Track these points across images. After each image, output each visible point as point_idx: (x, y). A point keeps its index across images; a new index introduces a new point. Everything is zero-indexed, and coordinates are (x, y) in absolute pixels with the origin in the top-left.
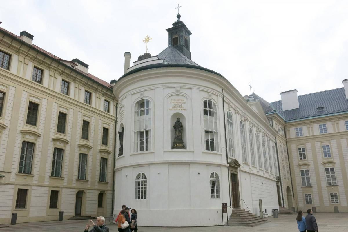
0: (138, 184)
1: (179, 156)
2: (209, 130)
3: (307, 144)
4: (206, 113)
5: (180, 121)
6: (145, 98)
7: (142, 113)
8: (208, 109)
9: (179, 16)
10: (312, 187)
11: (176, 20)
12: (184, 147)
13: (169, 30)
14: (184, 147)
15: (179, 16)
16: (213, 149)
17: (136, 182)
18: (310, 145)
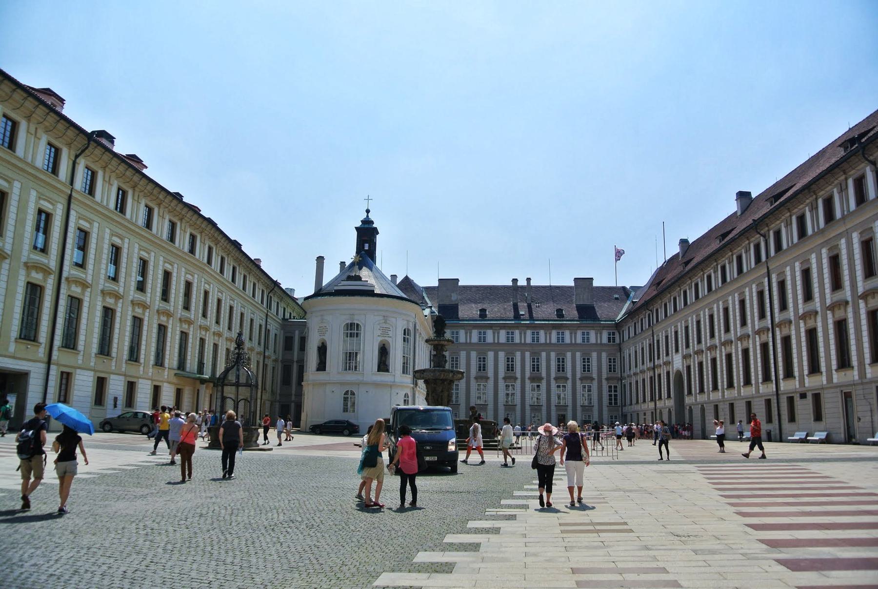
0: (346, 399)
1: (383, 377)
2: (406, 356)
3: (461, 352)
4: (404, 341)
5: (387, 346)
6: (356, 322)
7: (351, 335)
8: (407, 336)
9: (368, 211)
10: (459, 405)
11: (364, 216)
12: (387, 371)
13: (356, 228)
14: (387, 371)
15: (368, 211)
16: (407, 373)
17: (344, 398)
18: (465, 354)
